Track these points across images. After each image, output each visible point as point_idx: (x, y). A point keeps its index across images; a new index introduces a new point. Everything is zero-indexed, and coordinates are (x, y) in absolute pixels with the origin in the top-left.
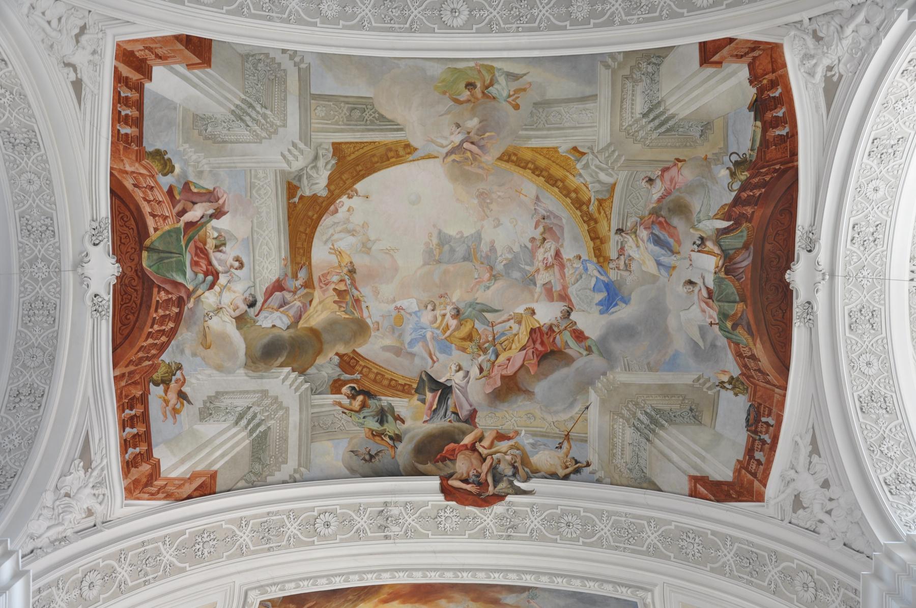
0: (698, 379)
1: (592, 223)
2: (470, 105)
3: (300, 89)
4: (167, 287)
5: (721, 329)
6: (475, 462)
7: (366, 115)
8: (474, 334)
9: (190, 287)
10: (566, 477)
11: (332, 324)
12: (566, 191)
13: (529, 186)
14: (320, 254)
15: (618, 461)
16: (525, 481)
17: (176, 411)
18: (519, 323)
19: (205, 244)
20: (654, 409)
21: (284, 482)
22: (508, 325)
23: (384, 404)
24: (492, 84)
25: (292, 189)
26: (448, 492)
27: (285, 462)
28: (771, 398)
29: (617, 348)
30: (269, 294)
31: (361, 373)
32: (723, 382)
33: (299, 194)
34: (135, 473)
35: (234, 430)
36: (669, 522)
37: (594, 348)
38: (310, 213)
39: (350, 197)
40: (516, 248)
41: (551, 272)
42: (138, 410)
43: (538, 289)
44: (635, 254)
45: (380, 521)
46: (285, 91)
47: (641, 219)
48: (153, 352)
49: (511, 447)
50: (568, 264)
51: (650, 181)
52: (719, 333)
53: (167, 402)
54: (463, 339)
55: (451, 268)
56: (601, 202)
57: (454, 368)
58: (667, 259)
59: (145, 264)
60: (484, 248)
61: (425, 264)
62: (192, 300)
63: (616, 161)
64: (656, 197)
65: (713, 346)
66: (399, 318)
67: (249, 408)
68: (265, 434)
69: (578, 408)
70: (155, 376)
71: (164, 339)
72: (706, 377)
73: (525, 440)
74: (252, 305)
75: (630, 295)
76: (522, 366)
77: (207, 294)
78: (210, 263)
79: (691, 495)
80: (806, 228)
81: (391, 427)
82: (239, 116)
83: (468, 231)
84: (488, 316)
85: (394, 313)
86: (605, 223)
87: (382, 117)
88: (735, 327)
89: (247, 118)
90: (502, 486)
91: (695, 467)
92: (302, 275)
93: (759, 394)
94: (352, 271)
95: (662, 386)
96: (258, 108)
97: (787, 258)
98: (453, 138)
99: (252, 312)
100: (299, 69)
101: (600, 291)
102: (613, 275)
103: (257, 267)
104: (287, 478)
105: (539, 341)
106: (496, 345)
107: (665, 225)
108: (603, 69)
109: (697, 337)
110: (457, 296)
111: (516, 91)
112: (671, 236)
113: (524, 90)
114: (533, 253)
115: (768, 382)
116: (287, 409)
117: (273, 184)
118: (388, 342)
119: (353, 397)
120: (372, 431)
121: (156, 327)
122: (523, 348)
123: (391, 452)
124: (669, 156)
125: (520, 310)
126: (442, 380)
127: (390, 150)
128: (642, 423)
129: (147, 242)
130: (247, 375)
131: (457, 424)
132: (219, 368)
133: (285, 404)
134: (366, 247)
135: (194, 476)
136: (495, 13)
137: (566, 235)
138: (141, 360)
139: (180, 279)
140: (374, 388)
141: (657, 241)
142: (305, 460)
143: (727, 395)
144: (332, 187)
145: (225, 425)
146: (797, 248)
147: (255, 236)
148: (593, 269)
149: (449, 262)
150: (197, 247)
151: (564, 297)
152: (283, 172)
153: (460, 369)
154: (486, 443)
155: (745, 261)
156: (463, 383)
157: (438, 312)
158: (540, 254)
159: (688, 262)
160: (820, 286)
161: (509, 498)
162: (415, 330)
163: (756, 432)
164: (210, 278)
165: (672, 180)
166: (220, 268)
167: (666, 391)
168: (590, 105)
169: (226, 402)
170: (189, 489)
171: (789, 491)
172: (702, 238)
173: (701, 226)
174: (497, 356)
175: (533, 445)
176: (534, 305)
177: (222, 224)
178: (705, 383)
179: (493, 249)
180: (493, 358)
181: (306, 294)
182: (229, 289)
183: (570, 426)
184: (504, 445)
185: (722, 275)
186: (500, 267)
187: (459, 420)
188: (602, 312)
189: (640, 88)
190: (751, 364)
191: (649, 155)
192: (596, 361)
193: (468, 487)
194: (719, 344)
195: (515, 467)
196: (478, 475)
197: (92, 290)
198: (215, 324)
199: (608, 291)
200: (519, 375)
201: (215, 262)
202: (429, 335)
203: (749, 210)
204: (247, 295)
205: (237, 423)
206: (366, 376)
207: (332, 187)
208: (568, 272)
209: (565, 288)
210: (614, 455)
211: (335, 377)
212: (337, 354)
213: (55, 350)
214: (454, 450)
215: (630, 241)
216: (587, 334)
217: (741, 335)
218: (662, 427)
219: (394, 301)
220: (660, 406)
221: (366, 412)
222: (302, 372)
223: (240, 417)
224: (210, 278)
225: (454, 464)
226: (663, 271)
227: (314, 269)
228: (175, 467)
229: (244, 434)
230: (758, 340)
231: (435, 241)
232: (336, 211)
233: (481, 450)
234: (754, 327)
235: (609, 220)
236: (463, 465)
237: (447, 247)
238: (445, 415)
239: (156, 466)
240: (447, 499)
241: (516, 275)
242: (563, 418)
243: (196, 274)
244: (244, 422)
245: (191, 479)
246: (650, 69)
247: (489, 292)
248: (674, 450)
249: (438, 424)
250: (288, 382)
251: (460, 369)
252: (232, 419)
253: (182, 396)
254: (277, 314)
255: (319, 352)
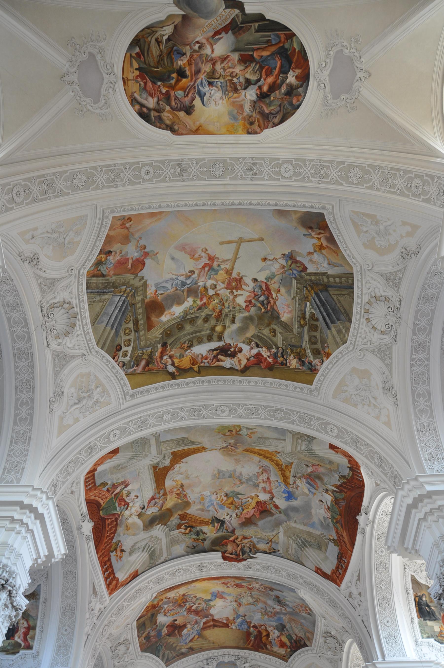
0: (322, 534)
1: (283, 472)
2: (230, 437)
3: (156, 442)
4: (110, 517)
5: (331, 521)
6: (235, 547)
7: (185, 442)
8: (234, 502)
9: (119, 513)
10: (270, 553)
11: (176, 506)
12: (272, 460)
13: (256, 458)
14: (169, 483)
15: (290, 552)
16: (254, 554)
17: (121, 557)
18: (252, 499)
19: (122, 497)
20: (304, 539)
21: (162, 563)
22: (247, 500)
23: (198, 529)
24: (240, 431)
25: (155, 468)
26: (225, 558)
27: (162, 556)
28: (347, 553)
29: (292, 514)
30: (149, 502)
31: (188, 520)
32: (330, 539)
33: (158, 468)
34: (111, 587)
35: (142, 554)
36: (307, 579)
37: (282, 512)
38: (163, 472)
39: (179, 464)
40: (251, 475)
41: (265, 483)
42: (108, 564)
43: (260, 489)
44: (299, 484)
45: (199, 568)
46: (150, 445)
47: (303, 475)
48: (109, 541)
49: (249, 542)
50: (273, 482)
51: (307, 466)
52: (331, 522)
53: (117, 556)
54: (229, 504)
55: (224, 480)
56: (286, 466)
57: (226, 514)
58: (312, 490)
59: (101, 515)
60: (237, 474)
61: (212, 479)
62: (120, 517)
63: (294, 457)
64: (309, 471)
65: (328, 525)
66: (203, 498)
67: (147, 544)
68: (154, 550)
69: (275, 532)
70: (111, 550)
71: (112, 535)
72: (324, 534)
73: (255, 540)
74: (143, 508)
75: (297, 498)
76: (253, 514)
77: (126, 512)
78: (125, 501)
79: (315, 572)
80: (366, 506)
81: (201, 537)
82: (132, 458)
83: (231, 468)
84: (240, 496)
85: (201, 497)
86: (288, 472)
87: (192, 442)
88: (337, 522)
89: (135, 458)
90: (245, 556)
91: (318, 564)
92: (162, 492)
93: (343, 549)
94: (182, 486)
95: (308, 532)
96: (139, 453)
97: (358, 512)
98: (223, 445)
99: (143, 511)
100: (155, 437)
101: (285, 493)
102: (291, 489)
103: (144, 496)
104: (163, 560)
105: (260, 506)
106: (243, 506)
107: (313, 480)
108: (289, 433)
109: (322, 520)
110: (226, 489)
111: (250, 433)
112: (315, 484)
113: (254, 433)
114: (258, 477)
115: (346, 547)
116: (161, 539)
117: (147, 469)
118: (199, 507)
119: (186, 529)
120: (194, 539)
121: (109, 533)
122: (254, 508)
123: (202, 544)
124: (316, 463)
125: (253, 495)
126: (221, 519)
127: (196, 450)
128: (300, 543)
129: (101, 508)
130: (144, 533)
131: (227, 534)
132: (134, 535)
133: (160, 538)
134: (187, 477)
135: (130, 575)
136: (241, 411)
137: (272, 473)
138: (106, 546)
139: (115, 512)
140: (194, 524)
141: (309, 484)
142: (169, 553)
143: (331, 545)
144: (172, 463)
145: (139, 554)
146: (361, 511)
147: (142, 486)
148: (282, 485)
149: (222, 478)
150: (120, 500)
151: (270, 492)
152: (151, 465)
153: (228, 514)
154: (239, 540)
155: (343, 503)
156: (229, 520)
157: (219, 495)
158: (261, 477)
159: (321, 494)
160: (368, 526)
161: (248, 560)
162: (209, 502)
163: (340, 562)
164: (126, 506)
165: (316, 469)
166: (129, 501)
167: (309, 534)
168: (283, 442)
169: (138, 545)
170: (129, 580)
171: (348, 590)
172: (327, 489)
173: (327, 486)
174: (243, 510)
175: (258, 542)
176: (258, 494)
177: (129, 488)
178: (324, 537)
179: (241, 474)
180: (241, 511)
181: (164, 498)
182: (134, 507)
183: (272, 537)
184: (246, 541)
185: (334, 504)
186: (244, 480)
187: (228, 532)
188: (286, 500)
189: (304, 443)
190: (341, 538)
191: (307, 459)
192: (283, 517)
193: (232, 556)
194: (330, 525)
195: (250, 549)
196: (236, 552)
197: (85, 534)
198: (130, 521)
199: (288, 494)
200: (252, 518)
201: (127, 501)
202: (215, 503)
203: (346, 490)
204: (141, 506)
205: (143, 551)
206: (191, 521)
207: (172, 463)
208: (272, 485)
209: (271, 490)
210: (288, 550)
211: (178, 523)
212: (178, 515)
213: (76, 557)
214: (227, 542)
215: (298, 481)
216: (279, 506)
217: (339, 526)
218: (307, 547)
219: (200, 493)
220: (307, 539)
221: (191, 533)
222: (165, 525)
223: (144, 548)
224: (126, 506)
225: (227, 547)
226: (311, 494)
227: (166, 489)
228: (124, 577)
229: (146, 554)
230: (345, 531)
231: (216, 472)
232: (174, 469)
233: (237, 542)
234: (344, 526)
235: (290, 472)
236: (230, 548)
237: (221, 474)
238: (223, 531)
239: (118, 580)
240: (224, 560)
241: (251, 483)
242: (270, 534)
243: (121, 507)
244: (146, 549)
245: (129, 577)
246: (309, 439)
247: (240, 488)
248: (310, 556)
249: (220, 534)
250: (160, 530)
251: (228, 514)
252: (141, 550)
253: (122, 551)
254: (153, 508)
255: (171, 516)
